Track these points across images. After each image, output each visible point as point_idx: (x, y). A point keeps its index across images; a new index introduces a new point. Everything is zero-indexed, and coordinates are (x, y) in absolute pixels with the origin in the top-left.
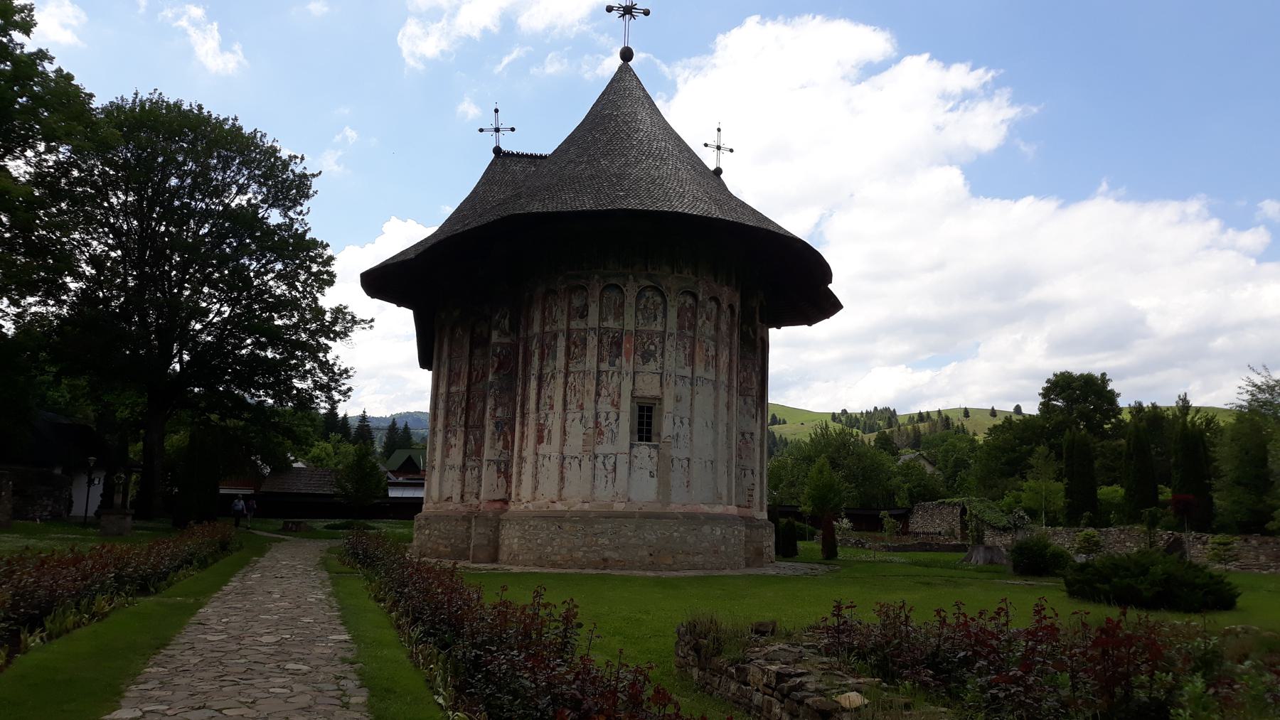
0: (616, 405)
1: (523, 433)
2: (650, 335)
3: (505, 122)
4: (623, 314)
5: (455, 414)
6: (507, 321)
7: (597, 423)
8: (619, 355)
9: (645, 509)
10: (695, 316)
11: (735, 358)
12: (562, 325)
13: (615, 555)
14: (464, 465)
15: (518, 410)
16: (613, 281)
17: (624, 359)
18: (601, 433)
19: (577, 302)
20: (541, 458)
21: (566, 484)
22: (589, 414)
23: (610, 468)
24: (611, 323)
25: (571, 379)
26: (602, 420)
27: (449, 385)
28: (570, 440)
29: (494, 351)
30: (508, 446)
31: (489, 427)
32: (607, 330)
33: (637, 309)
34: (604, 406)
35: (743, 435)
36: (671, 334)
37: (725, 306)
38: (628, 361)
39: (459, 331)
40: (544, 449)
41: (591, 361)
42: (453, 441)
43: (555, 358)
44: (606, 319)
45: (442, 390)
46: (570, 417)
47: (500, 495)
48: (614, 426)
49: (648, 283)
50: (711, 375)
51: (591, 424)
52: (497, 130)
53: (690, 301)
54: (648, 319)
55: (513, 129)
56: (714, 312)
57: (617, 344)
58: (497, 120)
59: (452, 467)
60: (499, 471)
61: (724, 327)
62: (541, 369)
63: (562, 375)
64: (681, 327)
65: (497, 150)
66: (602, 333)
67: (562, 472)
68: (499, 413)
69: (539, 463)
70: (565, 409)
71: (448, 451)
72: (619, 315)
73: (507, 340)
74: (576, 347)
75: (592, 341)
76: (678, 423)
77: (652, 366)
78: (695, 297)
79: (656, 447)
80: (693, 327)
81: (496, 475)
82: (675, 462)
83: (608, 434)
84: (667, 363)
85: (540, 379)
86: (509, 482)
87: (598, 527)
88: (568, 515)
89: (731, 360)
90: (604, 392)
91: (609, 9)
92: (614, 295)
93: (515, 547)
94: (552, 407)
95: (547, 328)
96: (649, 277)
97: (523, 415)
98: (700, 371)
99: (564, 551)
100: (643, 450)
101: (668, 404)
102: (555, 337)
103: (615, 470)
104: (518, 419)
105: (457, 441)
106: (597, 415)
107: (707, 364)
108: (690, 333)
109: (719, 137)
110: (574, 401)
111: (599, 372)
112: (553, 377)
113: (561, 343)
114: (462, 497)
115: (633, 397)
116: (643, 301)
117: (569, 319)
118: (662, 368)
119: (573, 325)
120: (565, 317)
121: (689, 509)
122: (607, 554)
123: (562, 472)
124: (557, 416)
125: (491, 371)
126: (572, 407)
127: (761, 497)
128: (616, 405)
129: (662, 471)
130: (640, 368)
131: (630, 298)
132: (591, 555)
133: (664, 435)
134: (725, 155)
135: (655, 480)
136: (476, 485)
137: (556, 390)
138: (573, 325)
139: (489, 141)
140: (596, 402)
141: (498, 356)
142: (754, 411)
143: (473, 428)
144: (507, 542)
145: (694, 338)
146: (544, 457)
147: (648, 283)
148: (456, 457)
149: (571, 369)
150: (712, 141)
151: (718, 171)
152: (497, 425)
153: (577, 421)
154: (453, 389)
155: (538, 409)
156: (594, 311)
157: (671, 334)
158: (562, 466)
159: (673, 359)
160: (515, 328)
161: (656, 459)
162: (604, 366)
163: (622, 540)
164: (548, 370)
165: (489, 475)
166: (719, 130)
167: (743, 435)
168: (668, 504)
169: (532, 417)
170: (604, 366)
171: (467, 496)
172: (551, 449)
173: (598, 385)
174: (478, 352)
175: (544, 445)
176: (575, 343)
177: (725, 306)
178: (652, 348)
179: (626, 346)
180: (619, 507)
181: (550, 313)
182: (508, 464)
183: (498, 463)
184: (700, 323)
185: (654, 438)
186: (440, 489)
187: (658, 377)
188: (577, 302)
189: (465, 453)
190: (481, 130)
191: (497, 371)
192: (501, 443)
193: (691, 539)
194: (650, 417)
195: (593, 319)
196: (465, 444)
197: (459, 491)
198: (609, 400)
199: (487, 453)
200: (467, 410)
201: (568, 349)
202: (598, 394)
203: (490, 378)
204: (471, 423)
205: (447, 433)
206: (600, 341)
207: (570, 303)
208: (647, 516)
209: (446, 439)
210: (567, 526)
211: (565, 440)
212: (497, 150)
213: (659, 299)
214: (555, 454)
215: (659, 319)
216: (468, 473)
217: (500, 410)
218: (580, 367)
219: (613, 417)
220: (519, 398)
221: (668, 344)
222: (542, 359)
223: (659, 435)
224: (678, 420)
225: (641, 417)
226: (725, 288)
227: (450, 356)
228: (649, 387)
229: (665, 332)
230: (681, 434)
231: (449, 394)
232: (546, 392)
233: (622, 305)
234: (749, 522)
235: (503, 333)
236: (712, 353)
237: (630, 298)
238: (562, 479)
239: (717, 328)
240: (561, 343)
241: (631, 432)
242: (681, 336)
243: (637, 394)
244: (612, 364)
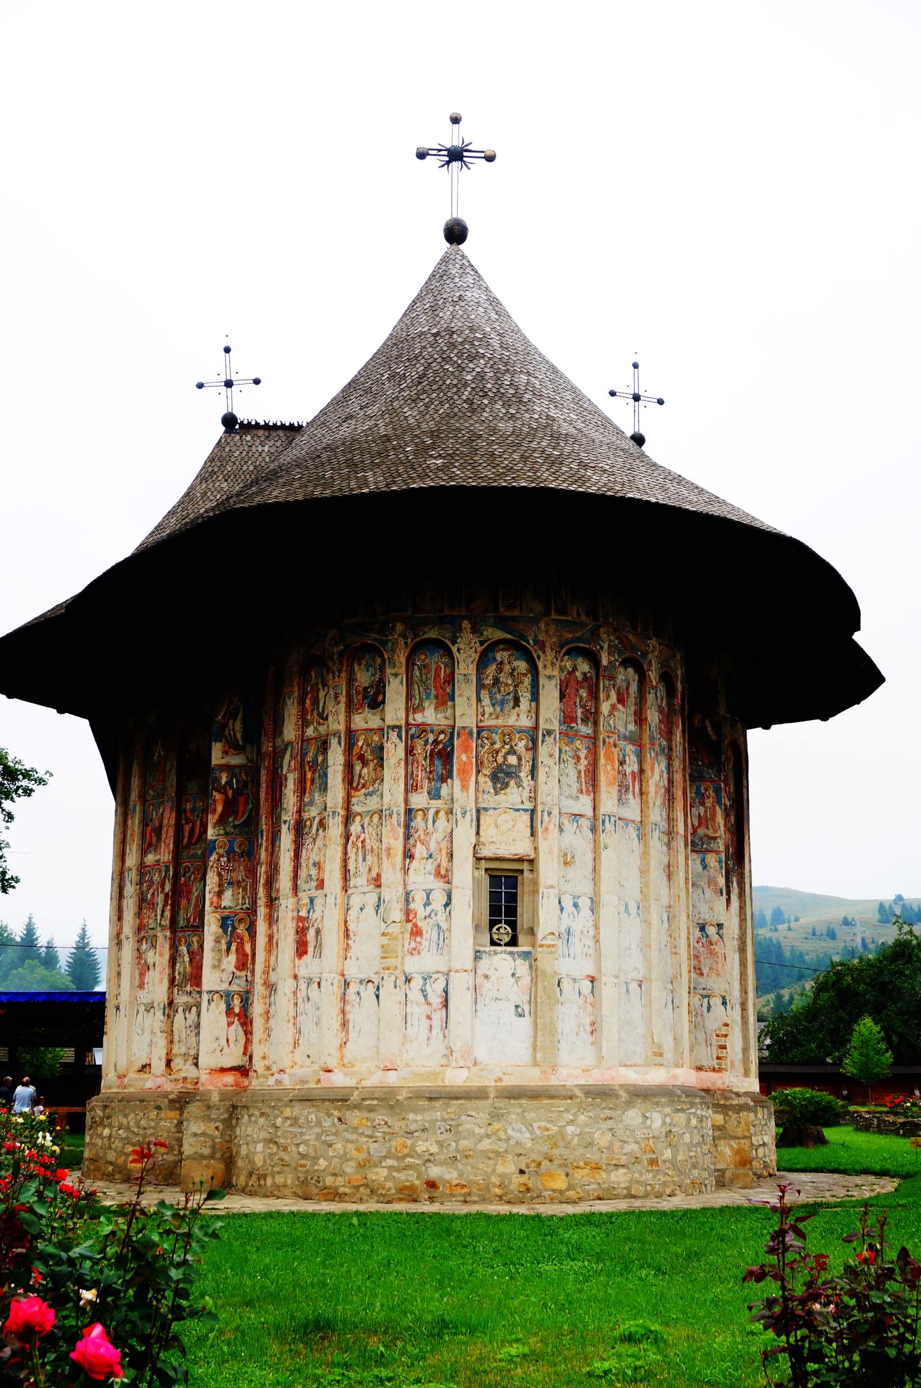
0: (444, 876)
1: (270, 937)
2: (508, 735)
3: (242, 370)
4: (452, 699)
5: (152, 905)
6: (238, 725)
7: (408, 914)
8: (446, 776)
9: (508, 1081)
10: (594, 695)
11: (678, 777)
12: (337, 723)
13: (450, 1175)
14: (171, 1003)
15: (261, 892)
16: (433, 634)
17: (457, 782)
18: (416, 932)
19: (364, 678)
20: (303, 985)
21: (353, 1035)
22: (392, 893)
23: (436, 1000)
24: (430, 716)
25: (355, 828)
26: (417, 905)
27: (144, 852)
28: (357, 947)
29: (218, 780)
30: (245, 963)
31: (212, 927)
32: (423, 729)
33: (480, 686)
34: (421, 877)
35: (702, 928)
36: (549, 733)
37: (653, 675)
38: (465, 787)
39: (159, 751)
40: (308, 966)
42: (151, 957)
43: (324, 788)
44: (419, 708)
45: (132, 860)
46: (356, 901)
47: (234, 1058)
48: (441, 918)
49: (499, 634)
50: (632, 810)
51: (397, 915)
52: (229, 384)
53: (584, 667)
54: (502, 703)
55: (257, 382)
56: (634, 687)
57: (443, 756)
58: (228, 365)
59: (150, 1008)
60: (229, 1011)
61: (653, 716)
62: (299, 811)
63: (339, 820)
64: (568, 718)
65: (229, 421)
66: (412, 734)
67: (343, 1012)
68: (228, 899)
69: (301, 995)
70: (345, 889)
71: (142, 975)
72: (446, 698)
73: (236, 760)
74: (365, 763)
75: (395, 751)
76: (568, 903)
77: (514, 795)
78: (594, 659)
79: (526, 955)
80: (592, 717)
81: (224, 1019)
82: (565, 984)
83: (429, 933)
84: (542, 788)
85: (299, 829)
86: (248, 1033)
87: (415, 1119)
88: (355, 1097)
89: (671, 781)
90: (419, 851)
91: (421, 155)
92: (435, 660)
93: (259, 1161)
94: (321, 885)
95: (310, 732)
96: (501, 623)
97: (272, 902)
98: (609, 802)
99: (350, 1168)
100: (502, 962)
101: (548, 871)
102: (324, 746)
103: (446, 1004)
104: (262, 911)
105: (158, 957)
106: (407, 897)
107: (623, 789)
108: (586, 730)
109: (636, 380)
110: (363, 869)
111: (409, 813)
112: (322, 825)
113: (336, 758)
114: (169, 1063)
115: (479, 859)
116: (492, 669)
117: (350, 709)
118: (533, 798)
119: (359, 722)
120: (342, 706)
121: (596, 1078)
122: (434, 1172)
123: (343, 1012)
124: (330, 900)
125: (212, 819)
126: (359, 881)
127: (745, 1050)
128: (444, 876)
129: (537, 1006)
130: (489, 800)
131: (466, 664)
132: (401, 1176)
133: (541, 932)
134: (648, 409)
135: (527, 1021)
136: (192, 1040)
137: (327, 850)
138: (359, 722)
139: (216, 405)
140: (406, 871)
141: (222, 790)
142: (722, 882)
143: (184, 929)
144: (244, 1150)
145: (594, 739)
146: (309, 981)
147: (499, 634)
148: (157, 987)
149: (356, 808)
150: (625, 387)
151: (639, 440)
152: (224, 926)
153: (370, 910)
154: (150, 858)
155: (295, 888)
156: (395, 692)
157: (549, 733)
158: (343, 999)
159: (557, 778)
160: (253, 737)
161: (526, 981)
162: (419, 800)
163: (464, 1143)
164: (312, 812)
165: (213, 1016)
166: (636, 366)
167: (702, 928)
168: (554, 1068)
169: (287, 905)
170: (419, 800)
171: (177, 1063)
172: (324, 964)
173: (407, 837)
174: (193, 787)
175: (307, 958)
176: (361, 758)
177: (653, 675)
178: (512, 760)
179: (460, 758)
180: (456, 1078)
181: (315, 701)
182: (246, 998)
183: (227, 996)
184: (605, 708)
185: (521, 938)
186: (127, 1050)
187: (526, 817)
188: (364, 678)
189: (172, 981)
190: (200, 386)
192: (233, 958)
193: (602, 1138)
194: (513, 898)
195: (395, 708)
196: (173, 961)
197: (163, 1053)
198: (430, 866)
199: (211, 979)
200: (176, 897)
201: (349, 767)
202: (408, 855)
203: (211, 833)
204: (182, 923)
205: (140, 941)
206: (409, 751)
207: (351, 680)
208: (514, 1094)
209: (139, 954)
210: (354, 1117)
211: (347, 948)
212: (229, 421)
213: (522, 666)
214: (331, 980)
215: (525, 704)
216: (179, 1018)
217: (228, 894)
218: (373, 803)
219: (439, 899)
220: (262, 870)
221: (543, 750)
222: (302, 789)
223: (532, 932)
224: (568, 903)
225: (494, 896)
226: (653, 642)
227: (143, 797)
228: (507, 838)
229: (536, 728)
230: (577, 928)
231: (142, 866)
232: (310, 854)
233: (451, 679)
234: (718, 1100)
235: (232, 747)
236: (632, 766)
237: (466, 664)
238: (345, 1024)
239: (640, 720)
240: (336, 758)
241: (477, 928)
242: (569, 735)
243: (486, 852)
244: (434, 795)
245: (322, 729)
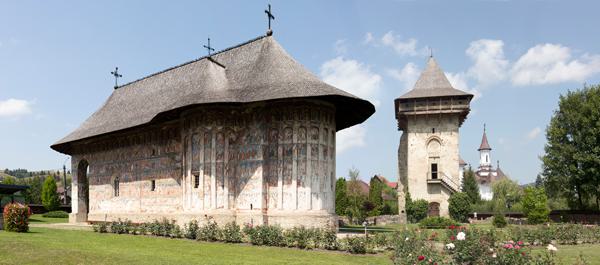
41: (321, 157)
85: (297, 161)
94: (305, 173)
102: (305, 145)
113: (309, 148)
156: (321, 137)
160: (272, 141)
191: (264, 155)
195: (321, 141)
245: (304, 142)
